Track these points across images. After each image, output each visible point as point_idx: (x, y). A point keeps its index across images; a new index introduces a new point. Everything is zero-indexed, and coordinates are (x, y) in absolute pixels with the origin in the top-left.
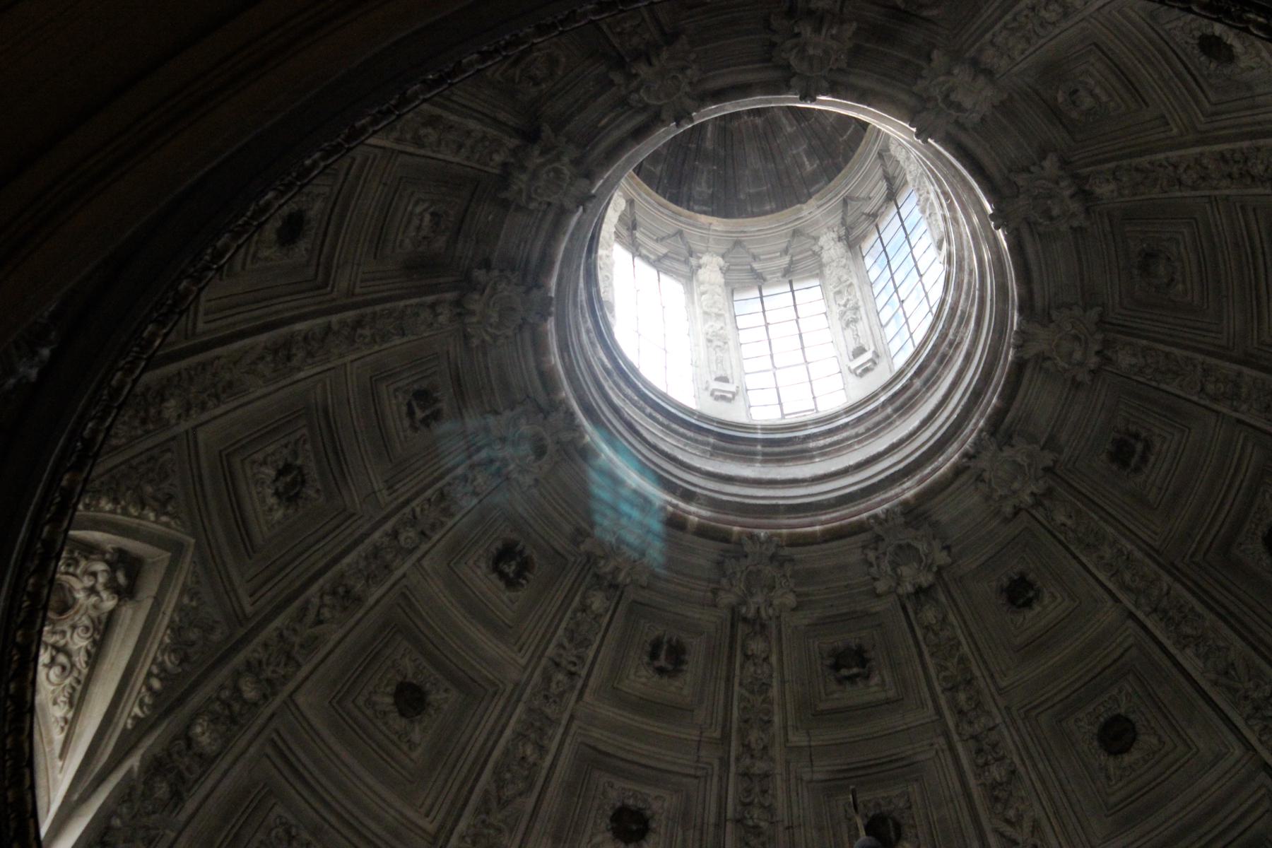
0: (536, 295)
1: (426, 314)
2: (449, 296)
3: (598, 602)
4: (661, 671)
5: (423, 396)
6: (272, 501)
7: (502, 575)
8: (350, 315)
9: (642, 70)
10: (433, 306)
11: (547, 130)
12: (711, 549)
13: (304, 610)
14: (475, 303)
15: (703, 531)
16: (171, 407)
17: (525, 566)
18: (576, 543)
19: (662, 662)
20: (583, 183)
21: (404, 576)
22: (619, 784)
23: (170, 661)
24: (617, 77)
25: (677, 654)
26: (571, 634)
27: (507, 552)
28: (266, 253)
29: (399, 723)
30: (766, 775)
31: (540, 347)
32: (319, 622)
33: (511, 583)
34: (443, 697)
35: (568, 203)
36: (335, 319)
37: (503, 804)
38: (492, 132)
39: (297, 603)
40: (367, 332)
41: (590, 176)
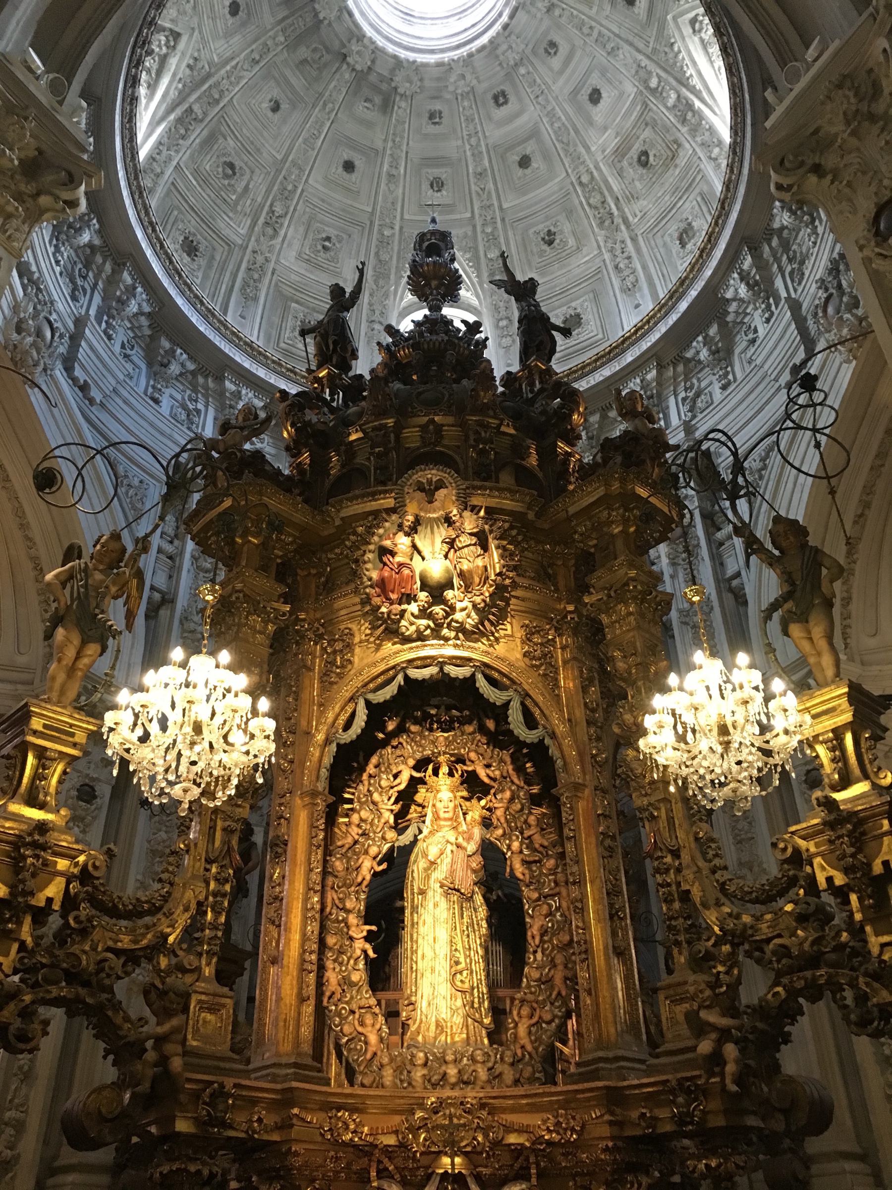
0: (405, 64)
1: (400, 112)
2: (398, 98)
3: (522, 71)
4: (555, 53)
5: (432, 116)
6: (439, 194)
7: (502, 105)
8: (390, 144)
9: (321, 16)
10: (399, 108)
11: (344, 51)
12: (520, 14)
13: (478, 194)
14: (401, 90)
15: (512, 16)
16: (387, 233)
17: (503, 94)
18: (503, 68)
19: (552, 51)
20: (366, 41)
21: (487, 145)
22: (583, 92)
23: (468, 256)
24: (326, 22)
25: (553, 44)
26: (530, 86)
27: (496, 98)
28: (354, 180)
29: (528, 171)
30: (600, 33)
31: (425, 65)
32: (483, 190)
33: (506, 102)
34: (529, 148)
35: (372, 47)
36: (389, 152)
37: (568, 144)
38: (337, 76)
39: (474, 195)
40: (398, 139)
41: (364, 36)
